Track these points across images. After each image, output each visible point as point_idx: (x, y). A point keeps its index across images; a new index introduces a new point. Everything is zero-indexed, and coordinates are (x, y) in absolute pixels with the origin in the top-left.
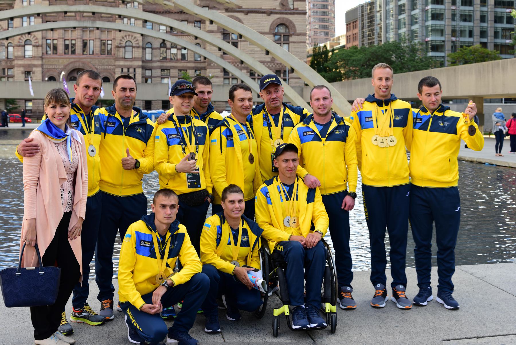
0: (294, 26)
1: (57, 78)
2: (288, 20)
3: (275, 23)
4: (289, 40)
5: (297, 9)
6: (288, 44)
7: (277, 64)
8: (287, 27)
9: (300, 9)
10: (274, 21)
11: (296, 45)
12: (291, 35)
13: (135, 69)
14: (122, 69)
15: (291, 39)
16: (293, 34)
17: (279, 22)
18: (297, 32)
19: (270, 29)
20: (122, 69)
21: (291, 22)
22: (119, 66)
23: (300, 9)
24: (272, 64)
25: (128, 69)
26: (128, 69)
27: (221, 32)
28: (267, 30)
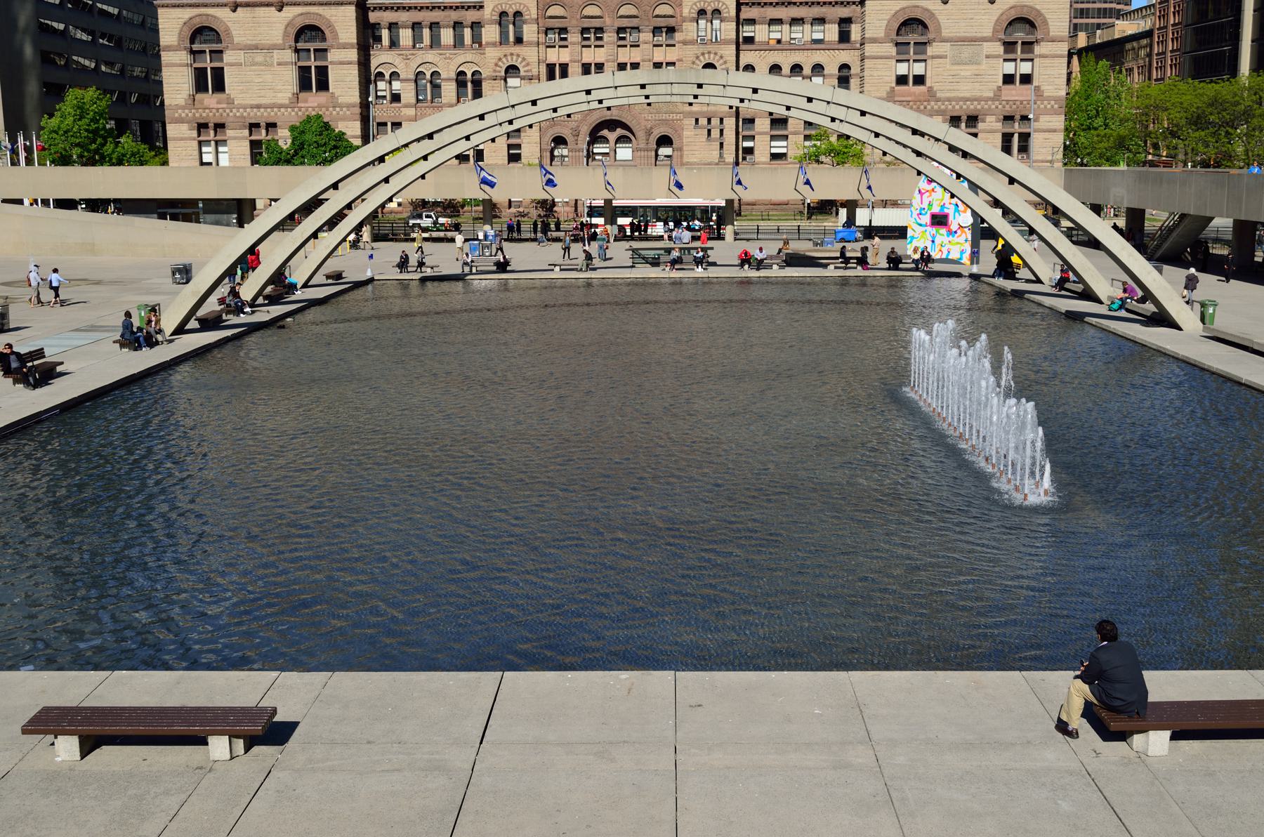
0: (1045, 22)
1: (569, 139)
3: (1004, 17)
8: (1032, 24)
11: (1047, 61)
13: (722, 120)
14: (697, 120)
16: (1042, 40)
19: (995, 31)
20: (697, 120)
22: (690, 114)
25: (709, 121)
26: (709, 121)
27: (892, 41)
28: (988, 32)
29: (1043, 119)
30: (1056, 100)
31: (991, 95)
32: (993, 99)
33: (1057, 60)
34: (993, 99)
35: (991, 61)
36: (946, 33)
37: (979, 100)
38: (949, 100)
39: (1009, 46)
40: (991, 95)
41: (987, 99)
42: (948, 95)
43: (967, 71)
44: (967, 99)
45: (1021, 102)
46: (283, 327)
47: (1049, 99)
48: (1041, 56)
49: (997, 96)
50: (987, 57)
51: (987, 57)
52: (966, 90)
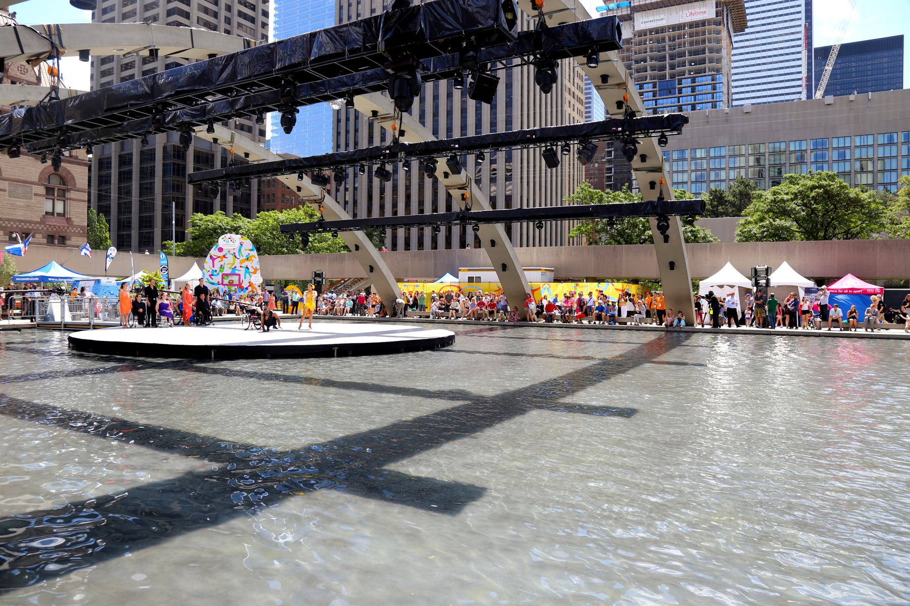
0: (73, 178)
4: (64, 196)
5: (76, 158)
7: (50, 226)
12: (68, 190)
15: (68, 195)
16: (71, 189)
19: (40, 179)
21: (68, 172)
28: (35, 179)
30: (82, 228)
32: (40, 223)
34: (40, 223)
36: (4, 175)
37: (30, 222)
38: (8, 220)
39: (49, 191)
41: (37, 223)
42: (8, 217)
43: (21, 202)
44: (21, 221)
46: (448, 498)
47: (77, 227)
48: (70, 199)
49: (42, 222)
50: (35, 195)
51: (35, 195)
52: (20, 215)
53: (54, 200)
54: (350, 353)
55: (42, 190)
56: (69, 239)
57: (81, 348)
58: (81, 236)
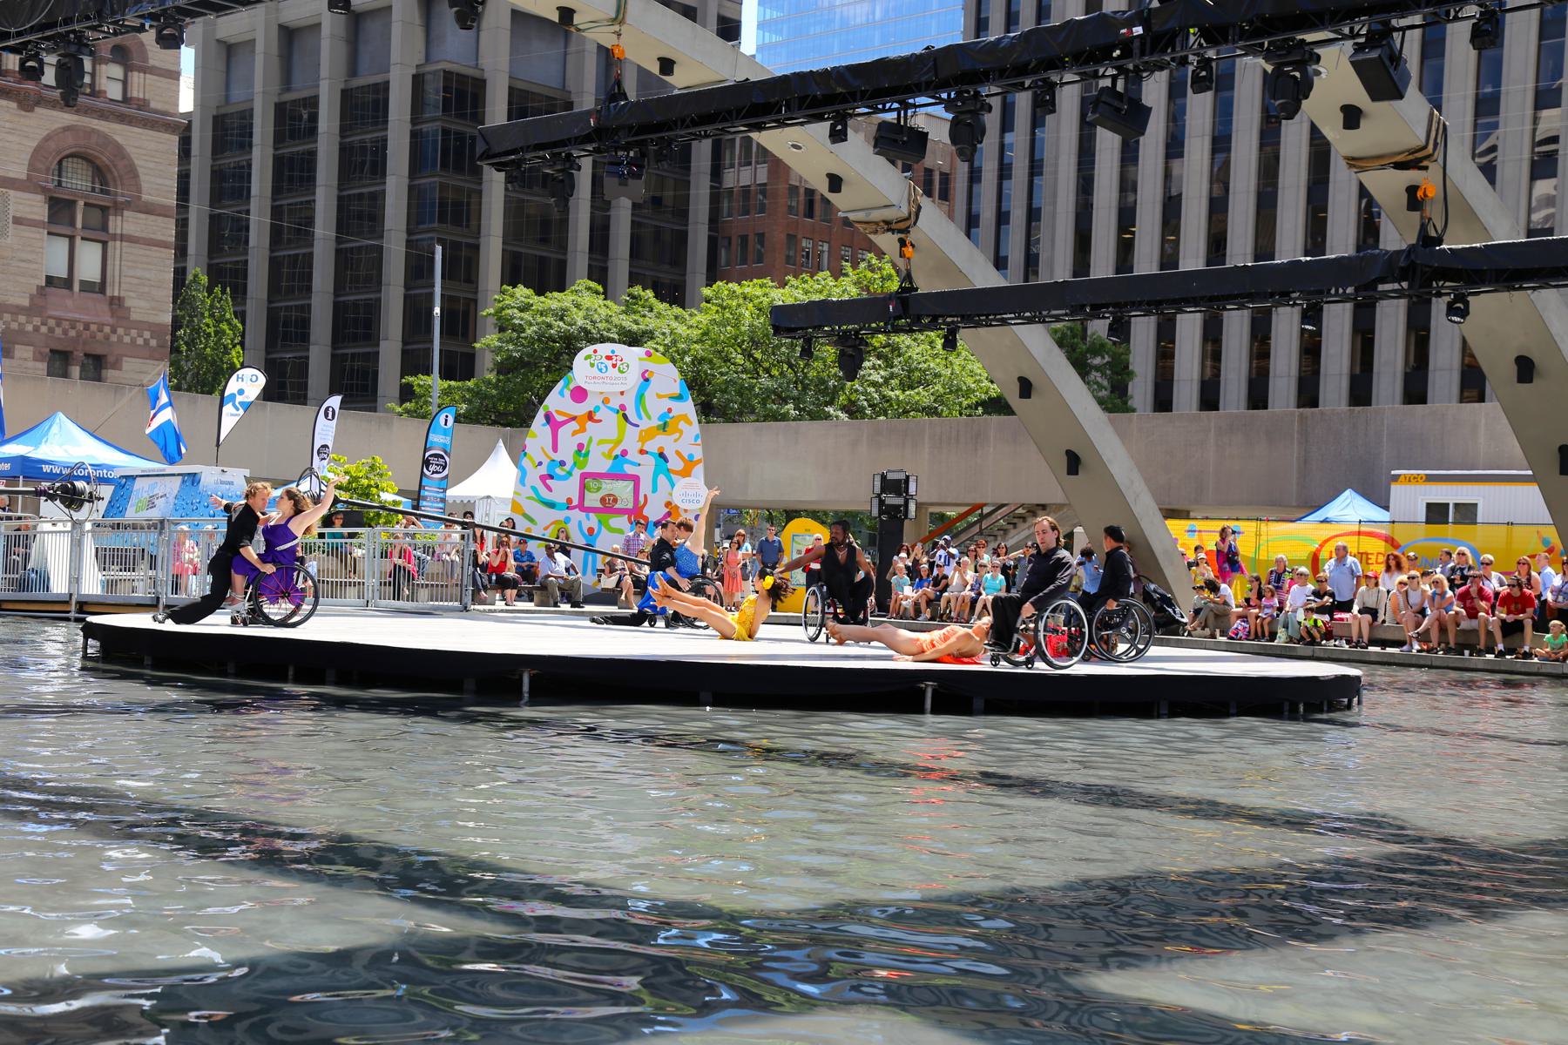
0: (133, 173)
2: (107, 140)
3: (52, 145)
4: (105, 228)
5: (143, 105)
6: (104, 244)
7: (59, 321)
9: (153, 105)
10: (47, 139)
11: (138, 250)
12: (118, 208)
15: (116, 224)
16: (128, 205)
17: (69, 143)
18: (145, 197)
21: (119, 151)
23: (153, 105)
24: (37, 321)
28: (19, 171)
29: (129, 364)
30: (155, 329)
31: (26, 303)
33: (156, 252)
35: (28, 232)
39: (60, 209)
40: (26, 303)
41: (17, 310)
45: (87, 326)
47: (141, 326)
48: (123, 238)
50: (18, 221)
51: (18, 221)
53: (72, 239)
54: (979, 703)
55: (37, 207)
56: (116, 365)
57: (120, 654)
58: (153, 355)
